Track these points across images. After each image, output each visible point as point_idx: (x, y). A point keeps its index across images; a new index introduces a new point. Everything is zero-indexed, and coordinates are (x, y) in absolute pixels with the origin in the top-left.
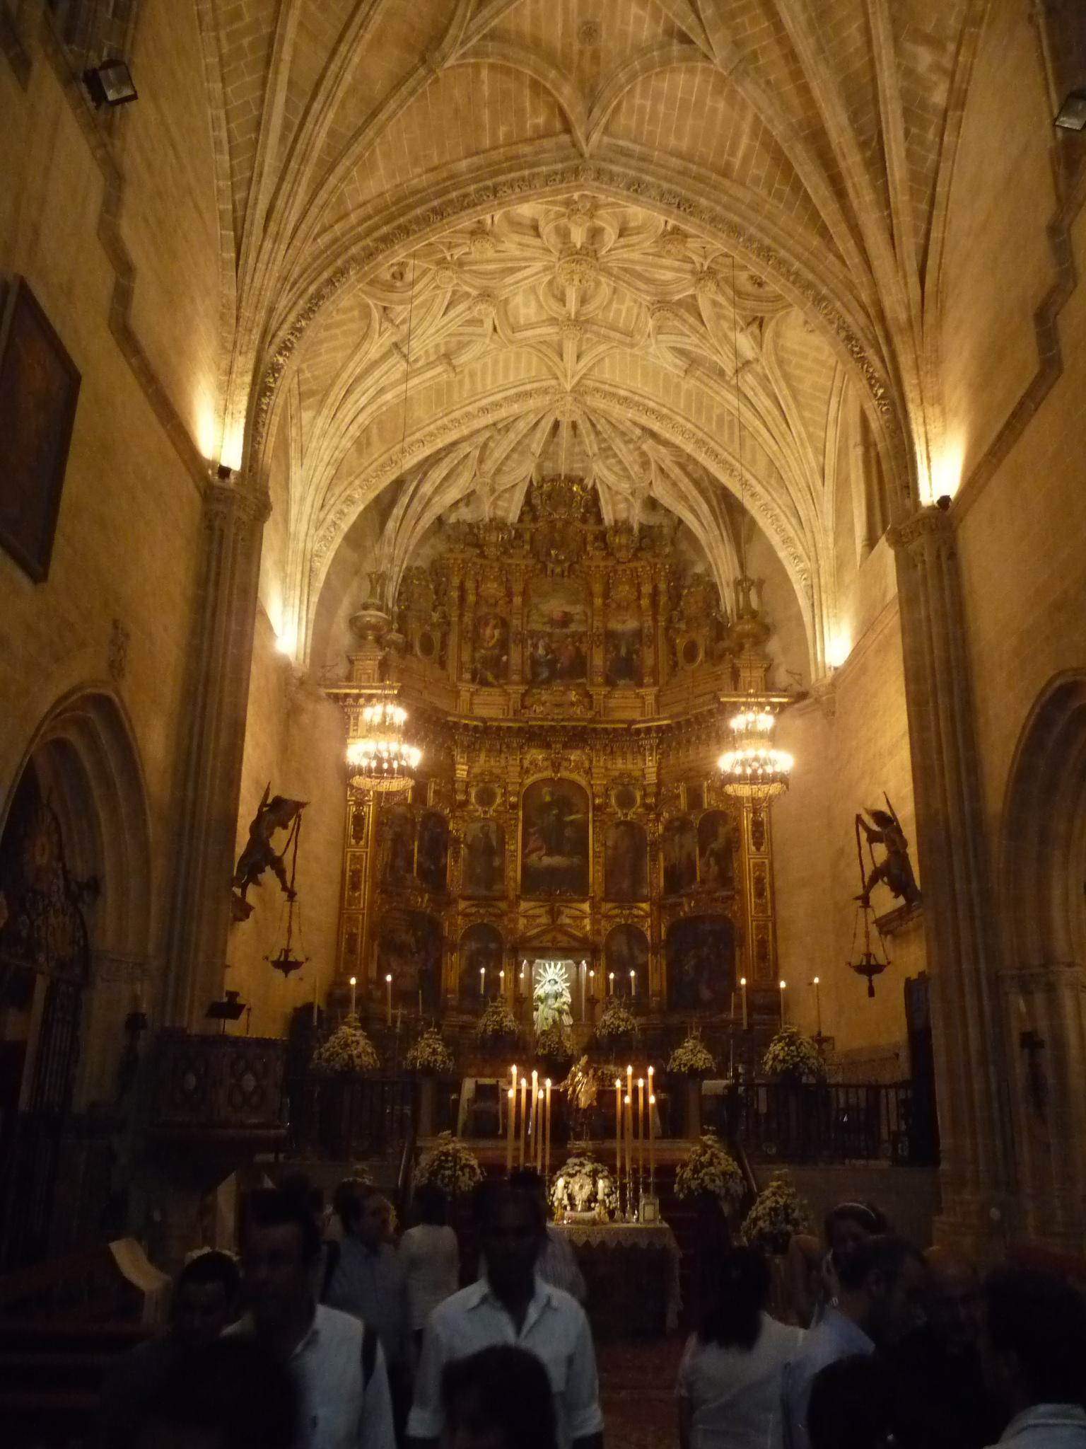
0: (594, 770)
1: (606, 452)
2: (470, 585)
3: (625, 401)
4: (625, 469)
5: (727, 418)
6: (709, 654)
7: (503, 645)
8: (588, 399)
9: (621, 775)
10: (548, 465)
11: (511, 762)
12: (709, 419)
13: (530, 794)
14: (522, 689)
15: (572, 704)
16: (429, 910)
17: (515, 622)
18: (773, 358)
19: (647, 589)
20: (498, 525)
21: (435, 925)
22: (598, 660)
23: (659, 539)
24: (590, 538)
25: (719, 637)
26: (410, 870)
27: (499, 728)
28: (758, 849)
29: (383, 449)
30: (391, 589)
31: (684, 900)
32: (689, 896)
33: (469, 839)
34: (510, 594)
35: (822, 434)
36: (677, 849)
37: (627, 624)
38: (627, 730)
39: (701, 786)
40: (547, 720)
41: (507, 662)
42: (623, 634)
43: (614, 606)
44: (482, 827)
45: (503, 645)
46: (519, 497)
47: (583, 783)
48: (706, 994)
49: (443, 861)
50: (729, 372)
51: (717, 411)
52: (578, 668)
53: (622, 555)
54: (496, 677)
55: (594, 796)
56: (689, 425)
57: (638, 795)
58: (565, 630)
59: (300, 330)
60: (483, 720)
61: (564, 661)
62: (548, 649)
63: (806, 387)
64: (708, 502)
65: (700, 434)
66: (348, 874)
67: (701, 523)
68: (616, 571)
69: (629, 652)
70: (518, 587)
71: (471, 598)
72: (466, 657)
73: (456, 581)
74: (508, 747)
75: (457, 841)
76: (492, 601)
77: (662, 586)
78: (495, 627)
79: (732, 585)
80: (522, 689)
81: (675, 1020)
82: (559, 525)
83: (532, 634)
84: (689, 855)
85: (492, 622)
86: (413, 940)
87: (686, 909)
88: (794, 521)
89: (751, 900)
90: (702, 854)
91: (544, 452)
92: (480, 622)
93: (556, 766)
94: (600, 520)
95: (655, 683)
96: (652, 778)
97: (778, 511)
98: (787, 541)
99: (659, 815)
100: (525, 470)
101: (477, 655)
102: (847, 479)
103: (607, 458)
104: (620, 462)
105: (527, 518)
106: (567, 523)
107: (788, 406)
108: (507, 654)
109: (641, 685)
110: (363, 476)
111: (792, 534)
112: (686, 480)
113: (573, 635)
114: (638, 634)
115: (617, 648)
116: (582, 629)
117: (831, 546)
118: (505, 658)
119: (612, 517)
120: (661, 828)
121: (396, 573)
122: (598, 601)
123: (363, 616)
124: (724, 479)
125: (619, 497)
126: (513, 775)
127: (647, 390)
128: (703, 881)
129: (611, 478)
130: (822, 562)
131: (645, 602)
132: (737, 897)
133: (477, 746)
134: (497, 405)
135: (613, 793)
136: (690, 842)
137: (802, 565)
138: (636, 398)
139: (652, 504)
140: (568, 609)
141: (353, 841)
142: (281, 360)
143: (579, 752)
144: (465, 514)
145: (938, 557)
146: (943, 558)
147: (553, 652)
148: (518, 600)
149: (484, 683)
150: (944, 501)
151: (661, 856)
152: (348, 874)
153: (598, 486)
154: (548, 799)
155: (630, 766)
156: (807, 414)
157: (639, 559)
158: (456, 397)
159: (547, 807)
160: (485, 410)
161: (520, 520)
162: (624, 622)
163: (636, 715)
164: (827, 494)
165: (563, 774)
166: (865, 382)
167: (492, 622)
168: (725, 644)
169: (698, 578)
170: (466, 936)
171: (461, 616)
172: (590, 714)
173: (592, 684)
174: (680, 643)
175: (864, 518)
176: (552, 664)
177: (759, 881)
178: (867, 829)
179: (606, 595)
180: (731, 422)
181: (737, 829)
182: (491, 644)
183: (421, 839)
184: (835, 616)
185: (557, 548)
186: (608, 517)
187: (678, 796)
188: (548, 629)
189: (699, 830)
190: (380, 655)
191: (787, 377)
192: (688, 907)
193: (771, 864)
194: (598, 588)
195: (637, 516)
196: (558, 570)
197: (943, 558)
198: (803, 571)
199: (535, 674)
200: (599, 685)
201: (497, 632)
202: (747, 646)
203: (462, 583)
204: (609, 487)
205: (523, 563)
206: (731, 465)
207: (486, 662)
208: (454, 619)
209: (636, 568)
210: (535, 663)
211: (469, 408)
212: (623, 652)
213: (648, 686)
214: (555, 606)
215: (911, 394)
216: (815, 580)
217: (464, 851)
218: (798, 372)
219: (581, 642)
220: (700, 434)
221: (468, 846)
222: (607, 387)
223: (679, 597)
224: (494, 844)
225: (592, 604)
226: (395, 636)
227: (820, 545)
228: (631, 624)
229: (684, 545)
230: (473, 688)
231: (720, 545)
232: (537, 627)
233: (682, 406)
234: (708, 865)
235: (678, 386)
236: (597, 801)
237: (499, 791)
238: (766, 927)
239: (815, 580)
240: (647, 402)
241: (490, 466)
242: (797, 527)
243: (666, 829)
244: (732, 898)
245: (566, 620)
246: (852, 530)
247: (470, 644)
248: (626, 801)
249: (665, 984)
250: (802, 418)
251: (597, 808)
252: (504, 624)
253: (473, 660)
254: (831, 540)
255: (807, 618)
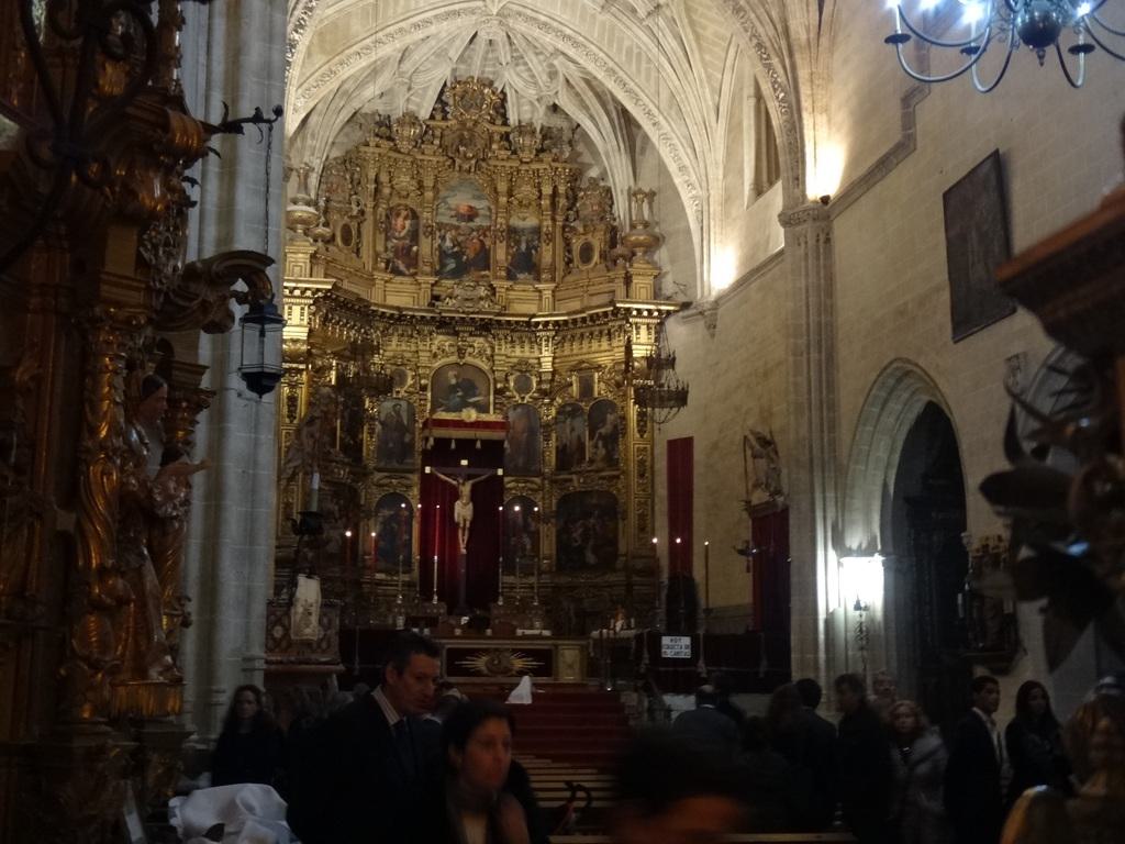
0: (496, 358)
1: (518, 59)
2: (384, 178)
3: (544, 26)
4: (533, 76)
5: (635, 51)
6: (603, 256)
7: (414, 236)
8: (511, 22)
9: (519, 364)
10: (462, 67)
11: (421, 347)
12: (620, 50)
13: (438, 374)
14: (432, 280)
15: (481, 298)
16: (349, 481)
17: (425, 215)
18: (682, 7)
19: (547, 190)
20: (411, 119)
21: (354, 493)
22: (501, 254)
23: (557, 139)
24: (497, 137)
25: (613, 244)
26: (334, 446)
27: (413, 317)
28: (642, 436)
29: (325, 59)
30: (313, 180)
31: (574, 477)
32: (579, 473)
33: (383, 417)
34: (421, 186)
35: (720, 76)
36: (568, 431)
37: (526, 221)
38: (528, 324)
39: (592, 376)
40: (458, 312)
41: (417, 253)
42: (523, 230)
43: (516, 202)
44: (395, 406)
45: (414, 236)
46: (432, 95)
47: (485, 366)
48: (591, 558)
49: (360, 437)
50: (642, 13)
51: (627, 43)
52: (483, 260)
53: (526, 156)
54: (408, 267)
55: (496, 381)
56: (601, 55)
57: (534, 380)
58: (471, 224)
59: (311, 9)
60: (398, 308)
61: (470, 253)
62: (456, 243)
63: (708, 33)
64: (608, 114)
65: (611, 64)
66: (283, 449)
67: (600, 132)
68: (518, 171)
69: (528, 248)
70: (429, 182)
71: (387, 191)
72: (380, 248)
73: (372, 175)
74: (419, 333)
75: (372, 418)
76: (405, 193)
77: (562, 189)
78: (406, 218)
79: (625, 193)
80: (432, 280)
81: (564, 580)
82: (470, 124)
83: (441, 226)
84: (579, 437)
85: (404, 213)
86: (336, 508)
87: (576, 484)
88: (689, 151)
89: (634, 479)
90: (591, 438)
91: (461, 59)
92: (392, 212)
93: (461, 352)
94: (505, 123)
95: (553, 280)
96: (547, 366)
97: (676, 141)
98: (682, 168)
99: (553, 400)
100: (442, 73)
101: (390, 245)
102: (740, 124)
103: (517, 65)
104: (529, 70)
105: (439, 116)
106: (476, 123)
107: (692, 50)
108: (417, 244)
109: (538, 280)
110: (306, 85)
111: (686, 162)
112: (590, 94)
113: (478, 229)
114: (537, 231)
115: (518, 243)
116: (486, 223)
117: (721, 177)
118: (415, 248)
119: (516, 118)
120: (553, 411)
121: (317, 164)
122: (503, 200)
123: (295, 211)
124: (629, 106)
125: (524, 100)
126: (424, 358)
127: (565, 17)
128: (592, 461)
129: (519, 84)
130: (712, 192)
131: (545, 203)
132: (622, 477)
133: (390, 331)
134: (428, 22)
135: (511, 378)
136: (581, 426)
137: (694, 192)
138: (555, 24)
139: (555, 108)
140: (474, 204)
141: (287, 420)
142: (296, 36)
143: (481, 340)
144: (381, 108)
145: (818, 241)
146: (821, 241)
147: (459, 244)
148: (429, 194)
149: (396, 272)
150: (825, 200)
151: (554, 435)
152: (283, 449)
153: (507, 90)
154: (454, 381)
155: (527, 354)
156: (707, 57)
157: (541, 161)
158: (391, 12)
159: (453, 389)
160: (417, 26)
161: (432, 117)
162: (524, 219)
163: (533, 309)
164: (720, 130)
165: (468, 359)
166: (770, 85)
167: (404, 213)
168: (620, 249)
169: (594, 182)
170: (381, 504)
171: (375, 207)
172: (497, 309)
173: (496, 278)
174: (577, 244)
175: (753, 163)
176: (457, 256)
177: (642, 463)
178: (752, 448)
179: (510, 194)
180: (639, 54)
181: (624, 418)
182: (402, 234)
183: (343, 417)
184: (721, 242)
185: (465, 146)
186: (513, 118)
187: (571, 384)
188: (454, 222)
189: (589, 415)
190: (312, 250)
191: (692, 23)
192: (577, 483)
193: (652, 449)
194: (502, 187)
195: (540, 118)
196: (466, 166)
197: (821, 241)
198: (695, 198)
199: (443, 265)
200: (501, 278)
201: (408, 223)
202: (639, 254)
203: (377, 176)
204: (516, 91)
205: (435, 159)
206: (636, 95)
207: (398, 252)
208: (369, 210)
209: (538, 170)
210: (443, 254)
211: (402, 24)
212: (523, 247)
213: (546, 281)
214: (461, 201)
215: (806, 103)
216: (705, 208)
217: (378, 427)
218: (703, 21)
219: (485, 236)
220: (611, 64)
221: (382, 423)
222: (529, 12)
223: (575, 199)
224: (405, 422)
225: (497, 201)
226: (321, 230)
227: (711, 177)
228: (532, 222)
229: (580, 148)
230: (387, 276)
231: (617, 154)
232: (445, 220)
233: (596, 35)
234: (596, 447)
235: (593, 16)
236: (499, 386)
237: (410, 374)
238: (646, 503)
239: (705, 208)
240: (564, 28)
241: (407, 66)
242: (692, 157)
243: (558, 413)
244: (618, 477)
245: (471, 215)
246: (741, 172)
247: (383, 236)
248: (523, 387)
249: (554, 547)
250: (702, 60)
251: (498, 392)
252: (414, 216)
253: (386, 249)
254: (721, 172)
255: (696, 239)
